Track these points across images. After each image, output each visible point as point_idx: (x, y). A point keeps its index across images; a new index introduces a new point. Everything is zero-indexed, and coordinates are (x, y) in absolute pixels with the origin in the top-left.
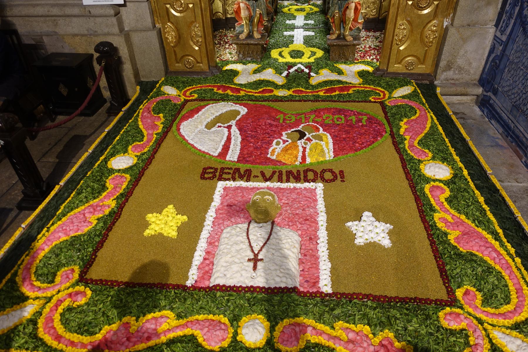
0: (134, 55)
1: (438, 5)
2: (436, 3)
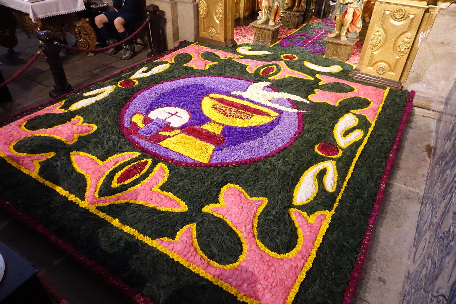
0: (177, 19)
1: (413, 18)
2: (411, 16)
